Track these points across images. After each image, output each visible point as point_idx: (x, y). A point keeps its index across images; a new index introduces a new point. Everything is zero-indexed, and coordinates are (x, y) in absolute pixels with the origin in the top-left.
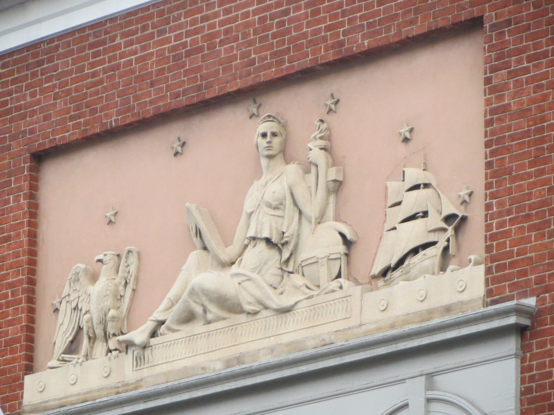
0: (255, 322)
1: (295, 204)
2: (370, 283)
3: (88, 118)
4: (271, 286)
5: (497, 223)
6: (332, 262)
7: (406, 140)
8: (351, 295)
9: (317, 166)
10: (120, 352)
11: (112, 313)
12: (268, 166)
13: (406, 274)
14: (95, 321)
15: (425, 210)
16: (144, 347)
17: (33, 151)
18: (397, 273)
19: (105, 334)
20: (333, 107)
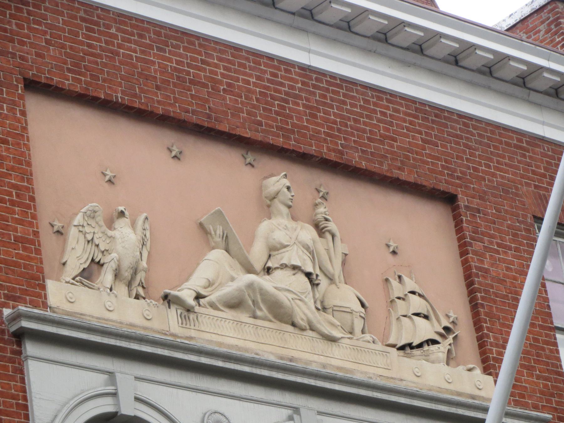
7: (394, 253)
8: (389, 353)
13: (426, 356)
18: (416, 352)
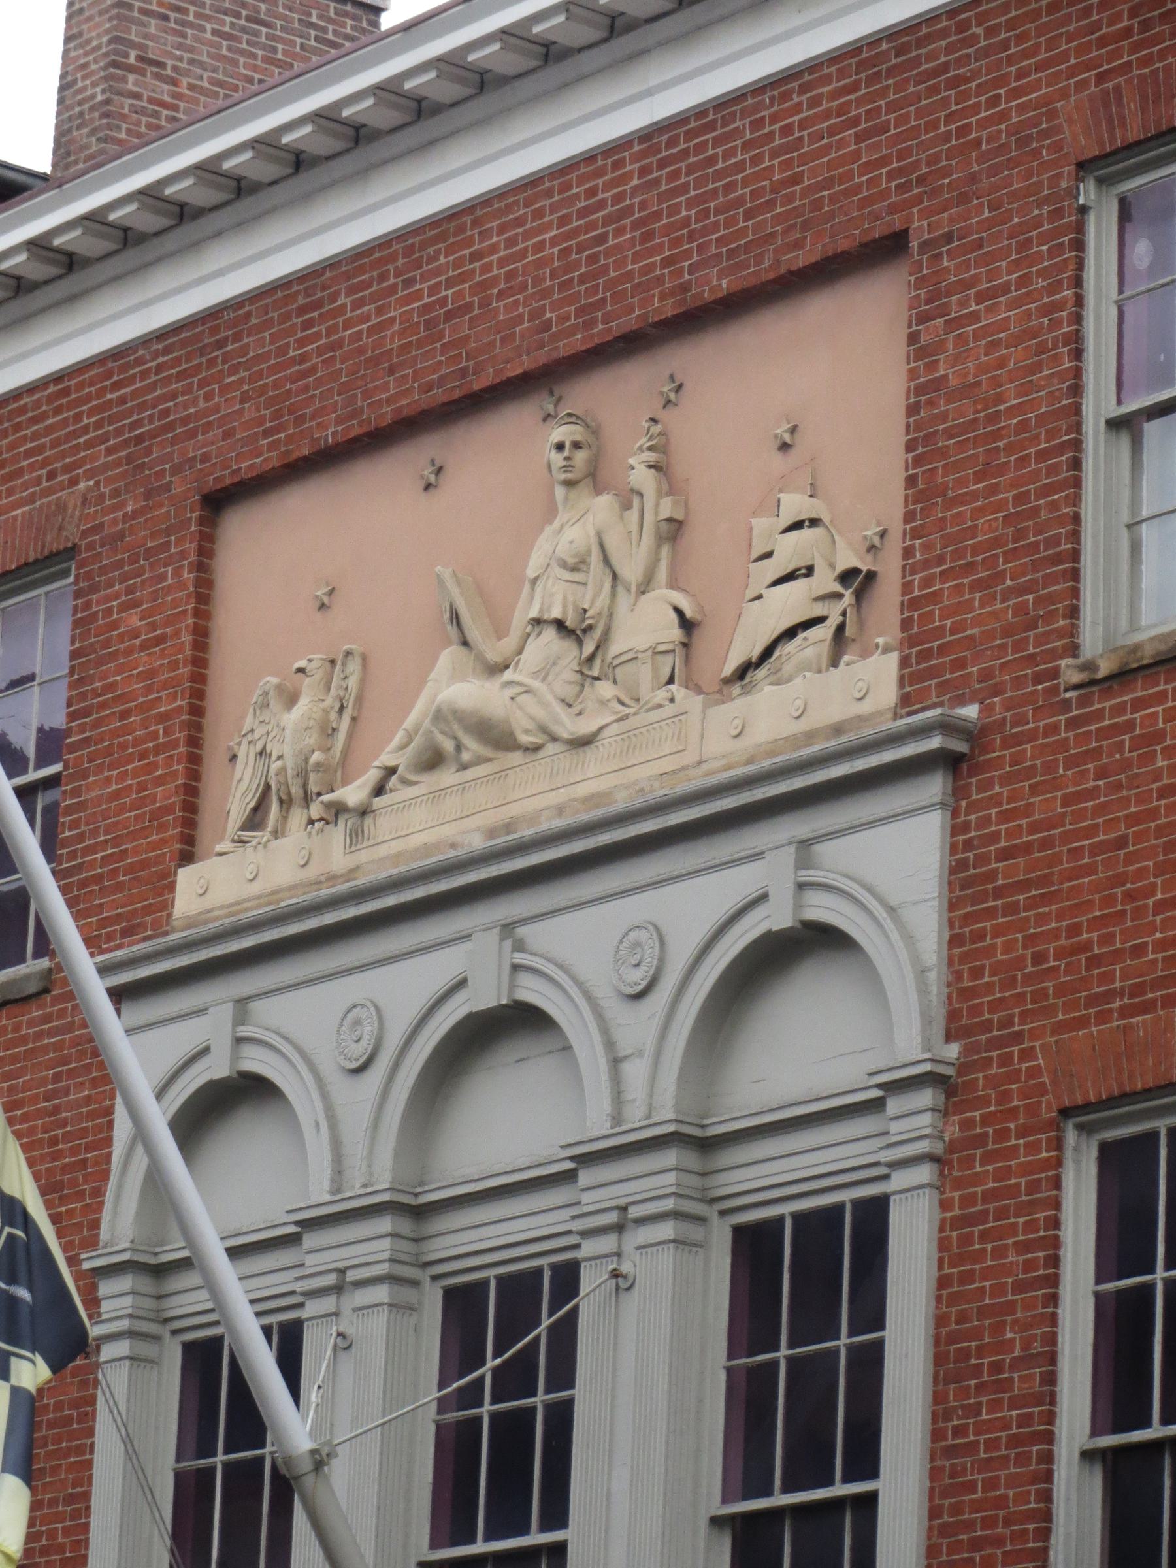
0: (536, 763)
1: (606, 561)
2: (720, 692)
3: (291, 431)
4: (563, 701)
5: (920, 579)
6: (659, 658)
7: (785, 447)
9: (641, 495)
10: (328, 823)
11: (316, 757)
12: (566, 499)
14: (290, 772)
15: (809, 563)
16: (364, 812)
17: (206, 491)
18: (761, 673)
19: (306, 792)
20: (672, 396)
